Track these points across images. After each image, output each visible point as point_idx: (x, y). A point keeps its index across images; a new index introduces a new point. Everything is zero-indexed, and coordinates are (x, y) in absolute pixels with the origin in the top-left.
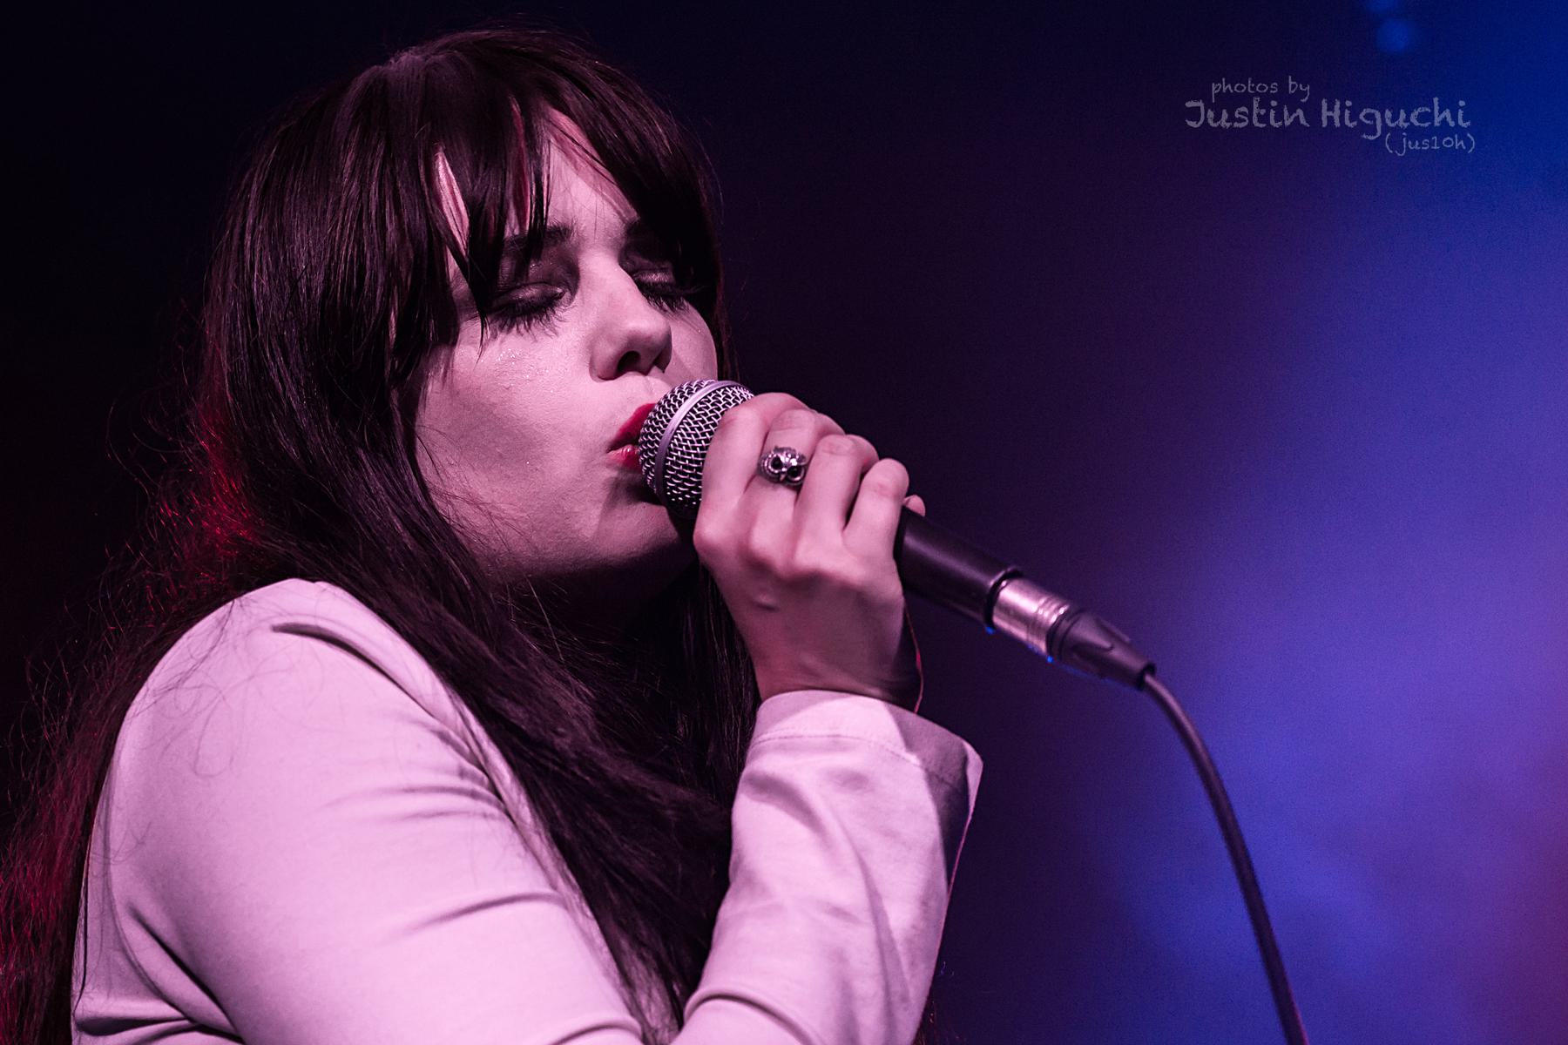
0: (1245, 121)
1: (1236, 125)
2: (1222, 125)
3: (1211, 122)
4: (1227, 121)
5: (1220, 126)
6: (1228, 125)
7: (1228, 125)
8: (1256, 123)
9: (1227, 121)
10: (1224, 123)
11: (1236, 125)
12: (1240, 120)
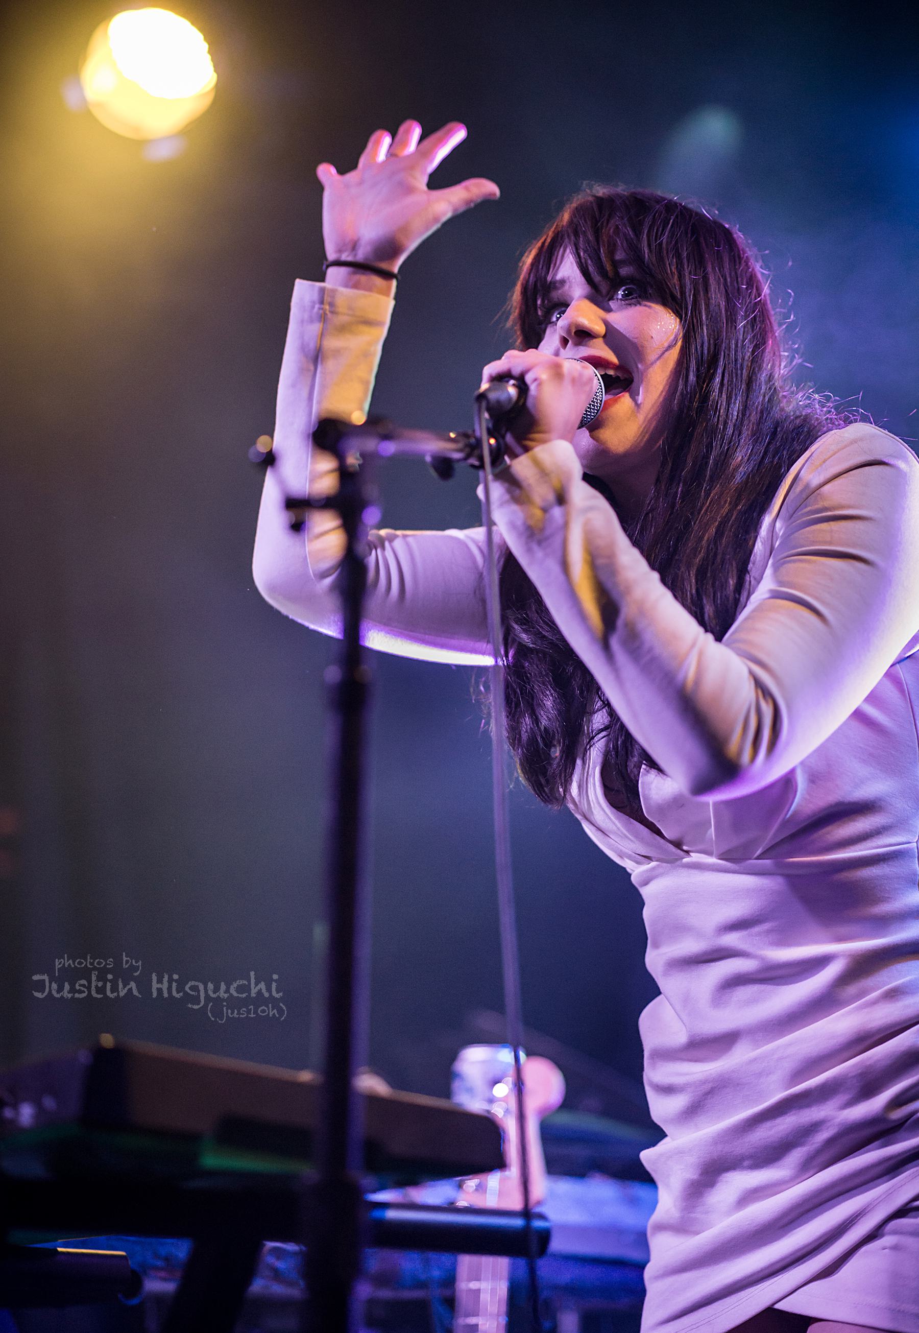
0: (84, 992)
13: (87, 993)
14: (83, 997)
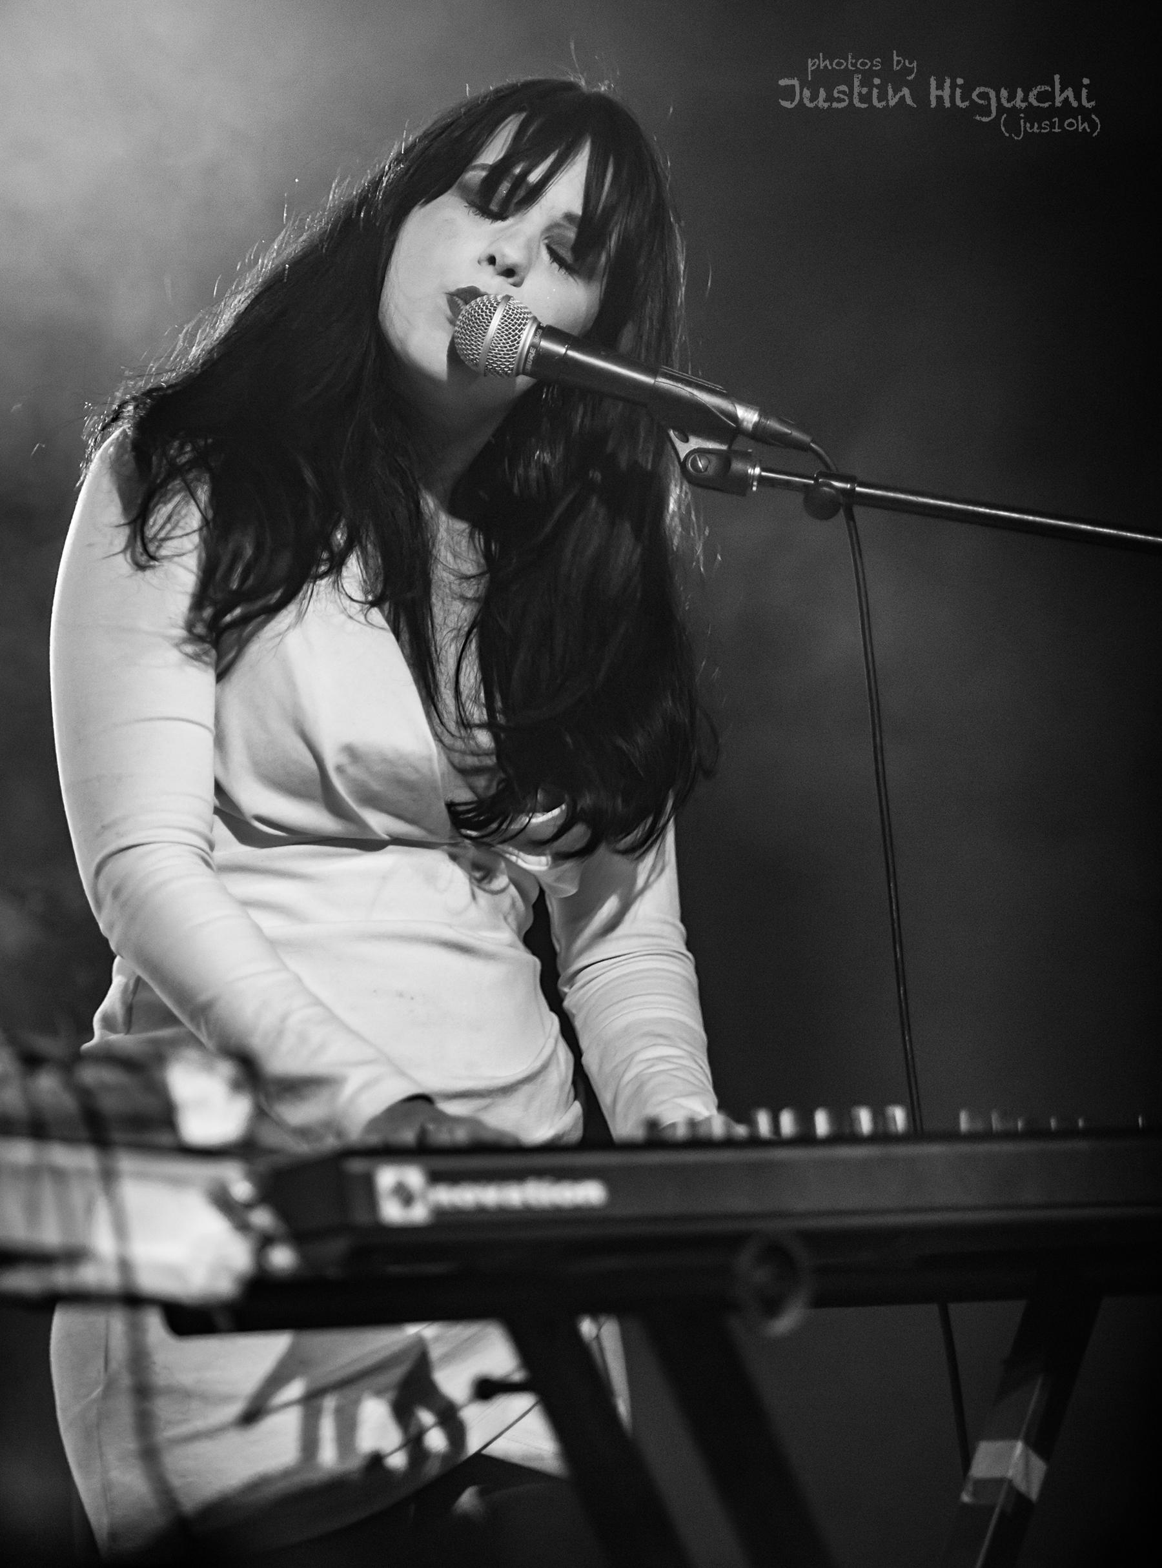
0: (844, 100)
1: (835, 105)
4: (824, 102)
5: (816, 106)
6: (826, 105)
7: (826, 105)
10: (821, 103)
11: (835, 105)
12: (840, 100)
13: (847, 101)
14: (843, 106)
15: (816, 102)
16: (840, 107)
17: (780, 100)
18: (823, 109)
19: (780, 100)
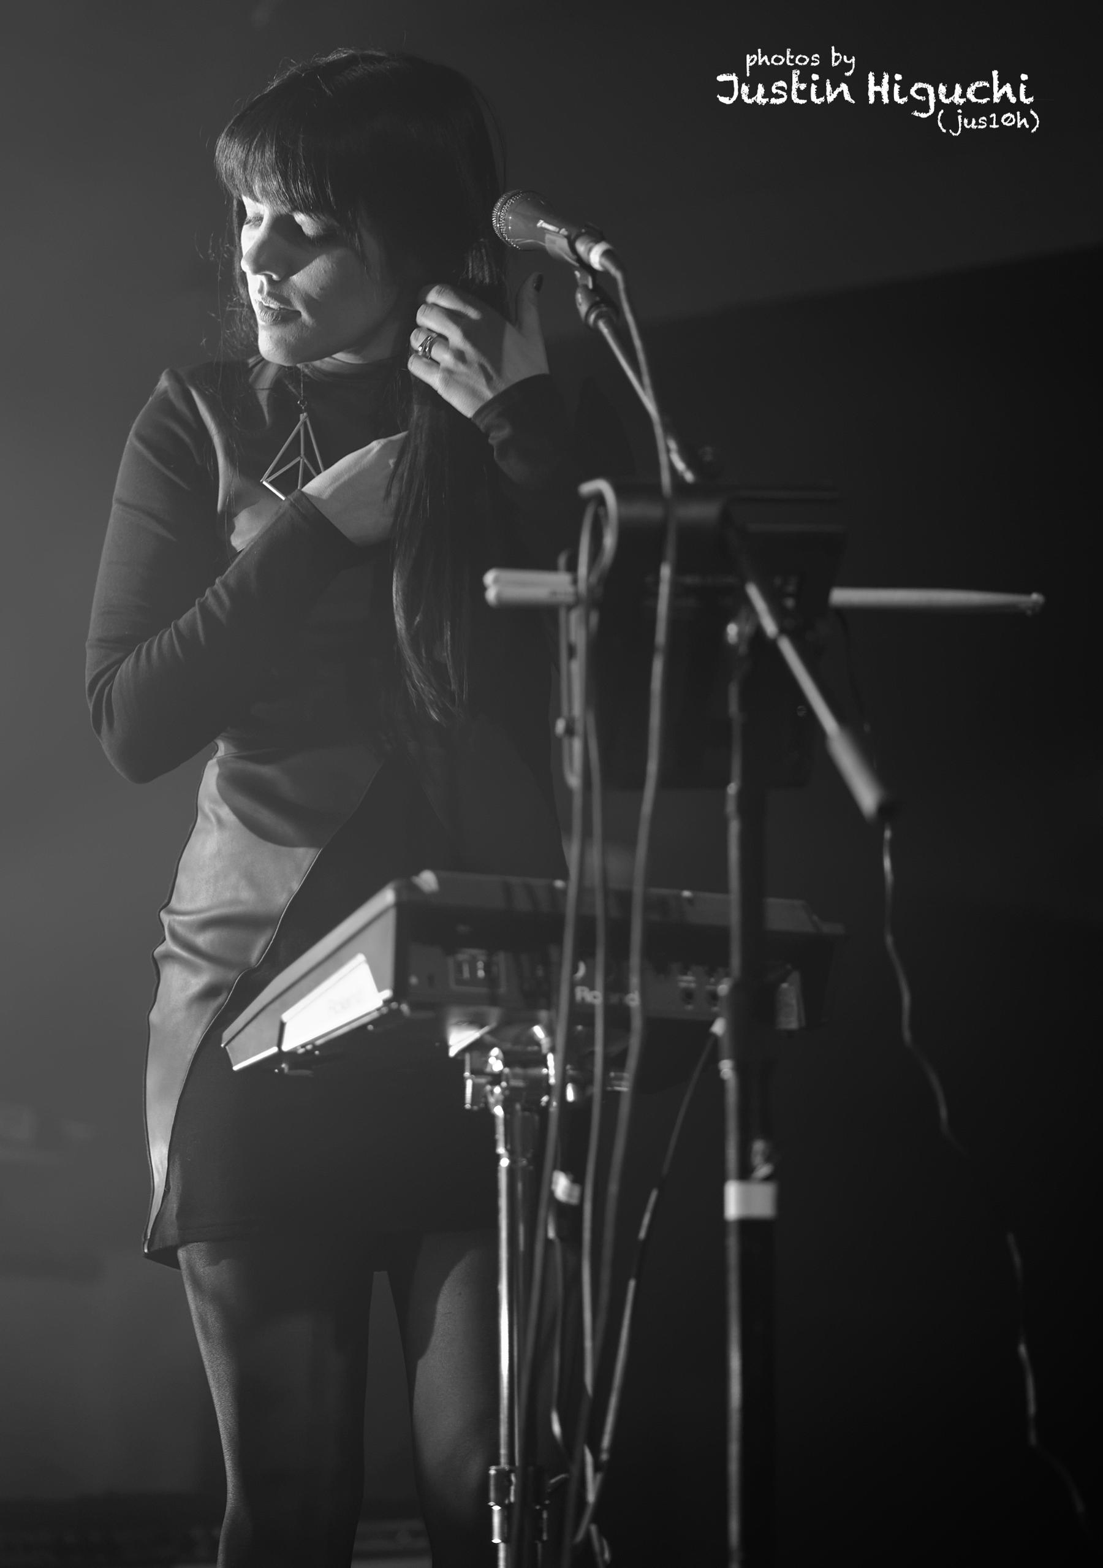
0: (782, 96)
1: (773, 101)
2: (758, 102)
3: (745, 98)
4: (763, 97)
5: (755, 102)
6: (765, 101)
7: (765, 101)
8: (796, 99)
9: (763, 97)
10: (760, 99)
11: (773, 101)
12: (778, 96)
13: (786, 97)
14: (781, 102)
15: (754, 98)
16: (778, 103)
17: (718, 96)
18: (761, 105)
19: (718, 96)
